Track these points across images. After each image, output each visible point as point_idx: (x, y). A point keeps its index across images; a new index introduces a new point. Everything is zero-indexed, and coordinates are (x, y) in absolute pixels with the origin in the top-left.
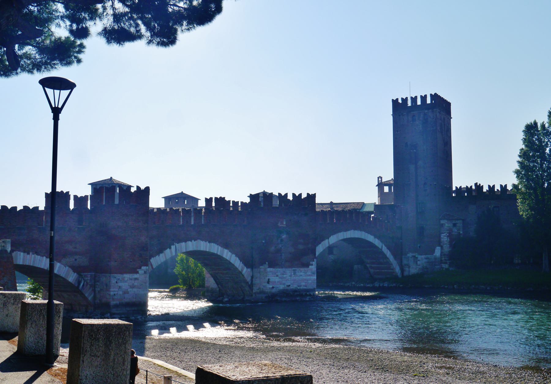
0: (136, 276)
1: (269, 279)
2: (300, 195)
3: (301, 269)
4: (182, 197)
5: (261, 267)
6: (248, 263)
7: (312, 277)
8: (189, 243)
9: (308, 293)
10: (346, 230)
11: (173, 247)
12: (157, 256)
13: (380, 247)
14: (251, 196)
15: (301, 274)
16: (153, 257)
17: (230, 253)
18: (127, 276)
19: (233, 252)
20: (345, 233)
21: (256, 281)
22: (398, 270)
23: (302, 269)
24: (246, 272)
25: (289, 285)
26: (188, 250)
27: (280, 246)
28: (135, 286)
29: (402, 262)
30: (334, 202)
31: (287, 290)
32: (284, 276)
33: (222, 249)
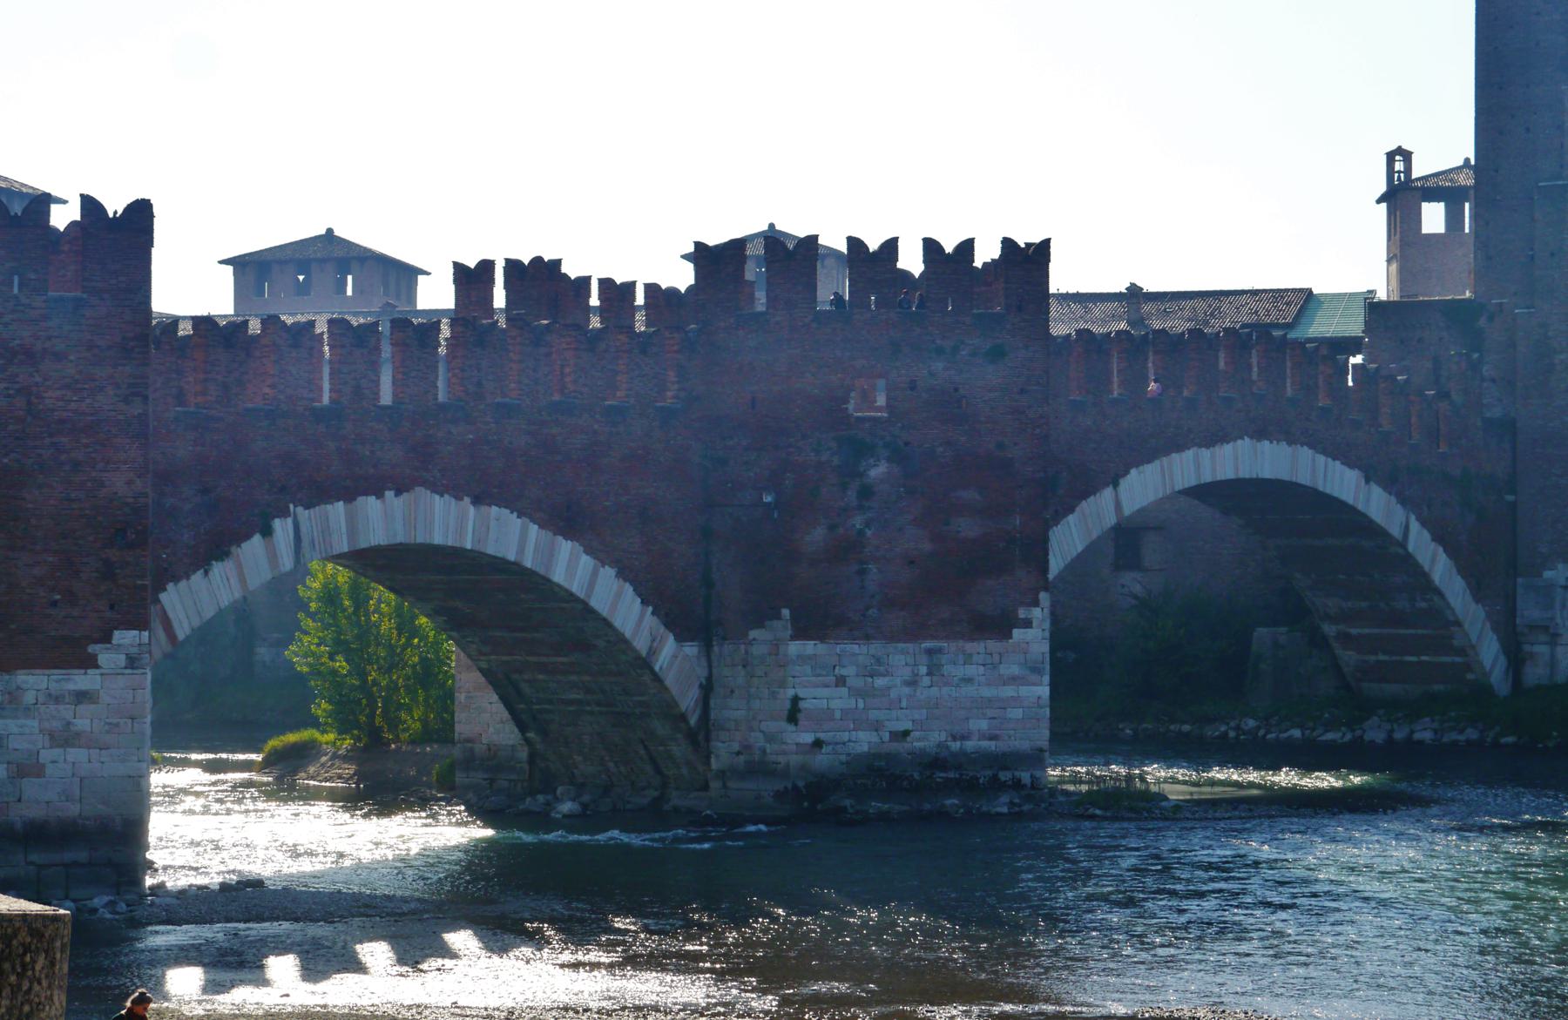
0: (82, 680)
1: (796, 700)
2: (967, 247)
3: (970, 647)
4: (328, 256)
5: (753, 634)
6: (688, 616)
7: (1024, 691)
8: (370, 505)
9: (1004, 776)
10: (1214, 438)
11: (282, 528)
12: (197, 577)
13: (1396, 532)
14: (702, 255)
15: (971, 670)
16: (176, 579)
17: (586, 561)
18: (33, 682)
19: (602, 555)
20: (1205, 453)
21: (730, 710)
22: (1490, 653)
23: (977, 647)
24: (673, 658)
25: (906, 733)
26: (363, 544)
27: (858, 521)
28: (78, 734)
29: (1512, 612)
30: (1150, 286)
31: (890, 757)
32: (880, 682)
33: (546, 535)
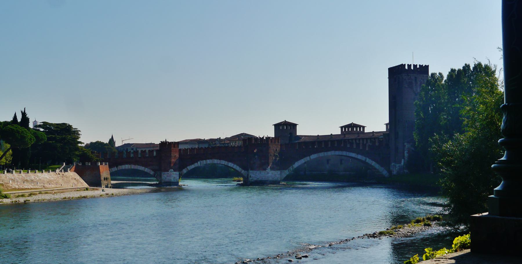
11: (199, 163)
17: (232, 164)
18: (166, 173)
